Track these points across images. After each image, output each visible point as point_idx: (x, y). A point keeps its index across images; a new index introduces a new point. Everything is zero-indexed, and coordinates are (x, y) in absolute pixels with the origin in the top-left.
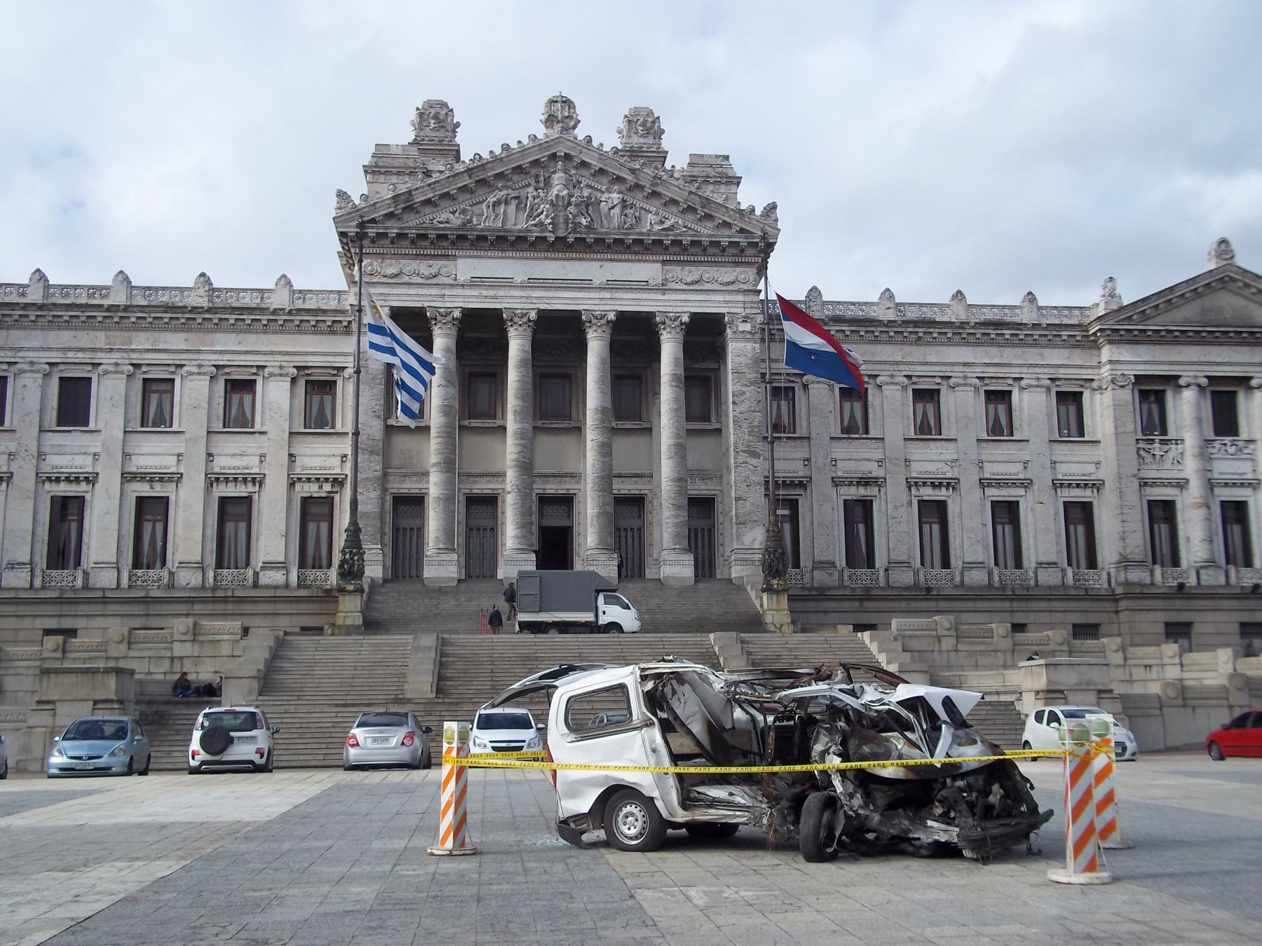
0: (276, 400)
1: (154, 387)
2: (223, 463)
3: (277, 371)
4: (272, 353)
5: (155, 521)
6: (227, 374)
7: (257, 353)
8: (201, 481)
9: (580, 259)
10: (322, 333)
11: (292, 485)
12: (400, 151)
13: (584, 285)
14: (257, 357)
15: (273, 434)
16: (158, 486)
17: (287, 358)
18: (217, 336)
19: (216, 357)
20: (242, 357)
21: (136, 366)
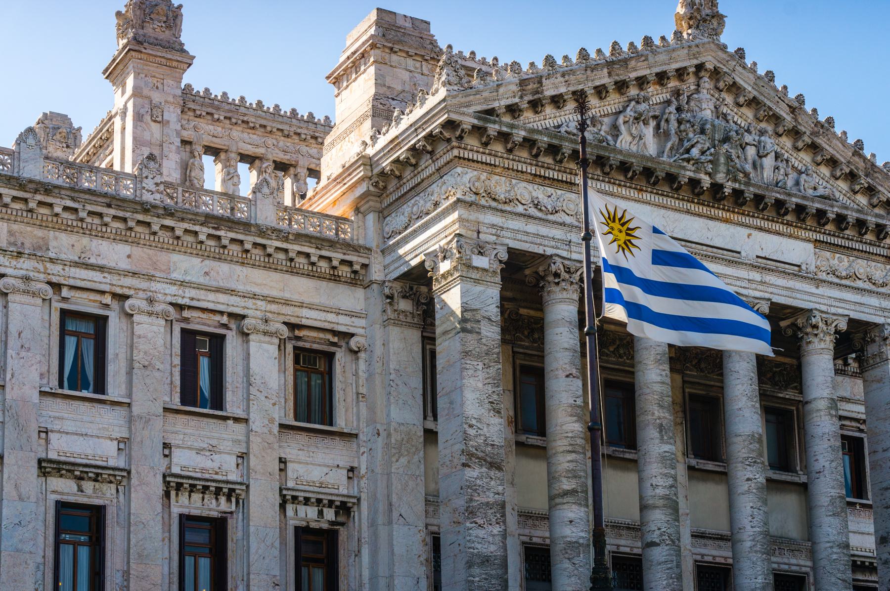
0: (261, 371)
1: (71, 326)
2: (184, 461)
3: (262, 327)
4: (254, 296)
5: (76, 544)
6: (186, 320)
7: (231, 292)
8: (158, 488)
9: (727, 221)
10: (321, 277)
11: (283, 507)
12: (408, 25)
13: (731, 257)
14: (234, 300)
15: (257, 423)
16: (88, 486)
17: (273, 307)
18: (175, 257)
19: (173, 289)
20: (212, 296)
21: (56, 287)
